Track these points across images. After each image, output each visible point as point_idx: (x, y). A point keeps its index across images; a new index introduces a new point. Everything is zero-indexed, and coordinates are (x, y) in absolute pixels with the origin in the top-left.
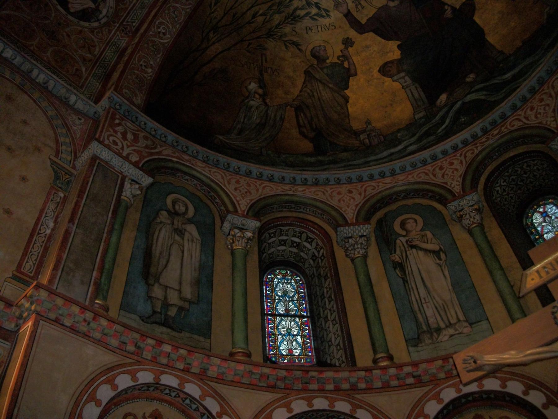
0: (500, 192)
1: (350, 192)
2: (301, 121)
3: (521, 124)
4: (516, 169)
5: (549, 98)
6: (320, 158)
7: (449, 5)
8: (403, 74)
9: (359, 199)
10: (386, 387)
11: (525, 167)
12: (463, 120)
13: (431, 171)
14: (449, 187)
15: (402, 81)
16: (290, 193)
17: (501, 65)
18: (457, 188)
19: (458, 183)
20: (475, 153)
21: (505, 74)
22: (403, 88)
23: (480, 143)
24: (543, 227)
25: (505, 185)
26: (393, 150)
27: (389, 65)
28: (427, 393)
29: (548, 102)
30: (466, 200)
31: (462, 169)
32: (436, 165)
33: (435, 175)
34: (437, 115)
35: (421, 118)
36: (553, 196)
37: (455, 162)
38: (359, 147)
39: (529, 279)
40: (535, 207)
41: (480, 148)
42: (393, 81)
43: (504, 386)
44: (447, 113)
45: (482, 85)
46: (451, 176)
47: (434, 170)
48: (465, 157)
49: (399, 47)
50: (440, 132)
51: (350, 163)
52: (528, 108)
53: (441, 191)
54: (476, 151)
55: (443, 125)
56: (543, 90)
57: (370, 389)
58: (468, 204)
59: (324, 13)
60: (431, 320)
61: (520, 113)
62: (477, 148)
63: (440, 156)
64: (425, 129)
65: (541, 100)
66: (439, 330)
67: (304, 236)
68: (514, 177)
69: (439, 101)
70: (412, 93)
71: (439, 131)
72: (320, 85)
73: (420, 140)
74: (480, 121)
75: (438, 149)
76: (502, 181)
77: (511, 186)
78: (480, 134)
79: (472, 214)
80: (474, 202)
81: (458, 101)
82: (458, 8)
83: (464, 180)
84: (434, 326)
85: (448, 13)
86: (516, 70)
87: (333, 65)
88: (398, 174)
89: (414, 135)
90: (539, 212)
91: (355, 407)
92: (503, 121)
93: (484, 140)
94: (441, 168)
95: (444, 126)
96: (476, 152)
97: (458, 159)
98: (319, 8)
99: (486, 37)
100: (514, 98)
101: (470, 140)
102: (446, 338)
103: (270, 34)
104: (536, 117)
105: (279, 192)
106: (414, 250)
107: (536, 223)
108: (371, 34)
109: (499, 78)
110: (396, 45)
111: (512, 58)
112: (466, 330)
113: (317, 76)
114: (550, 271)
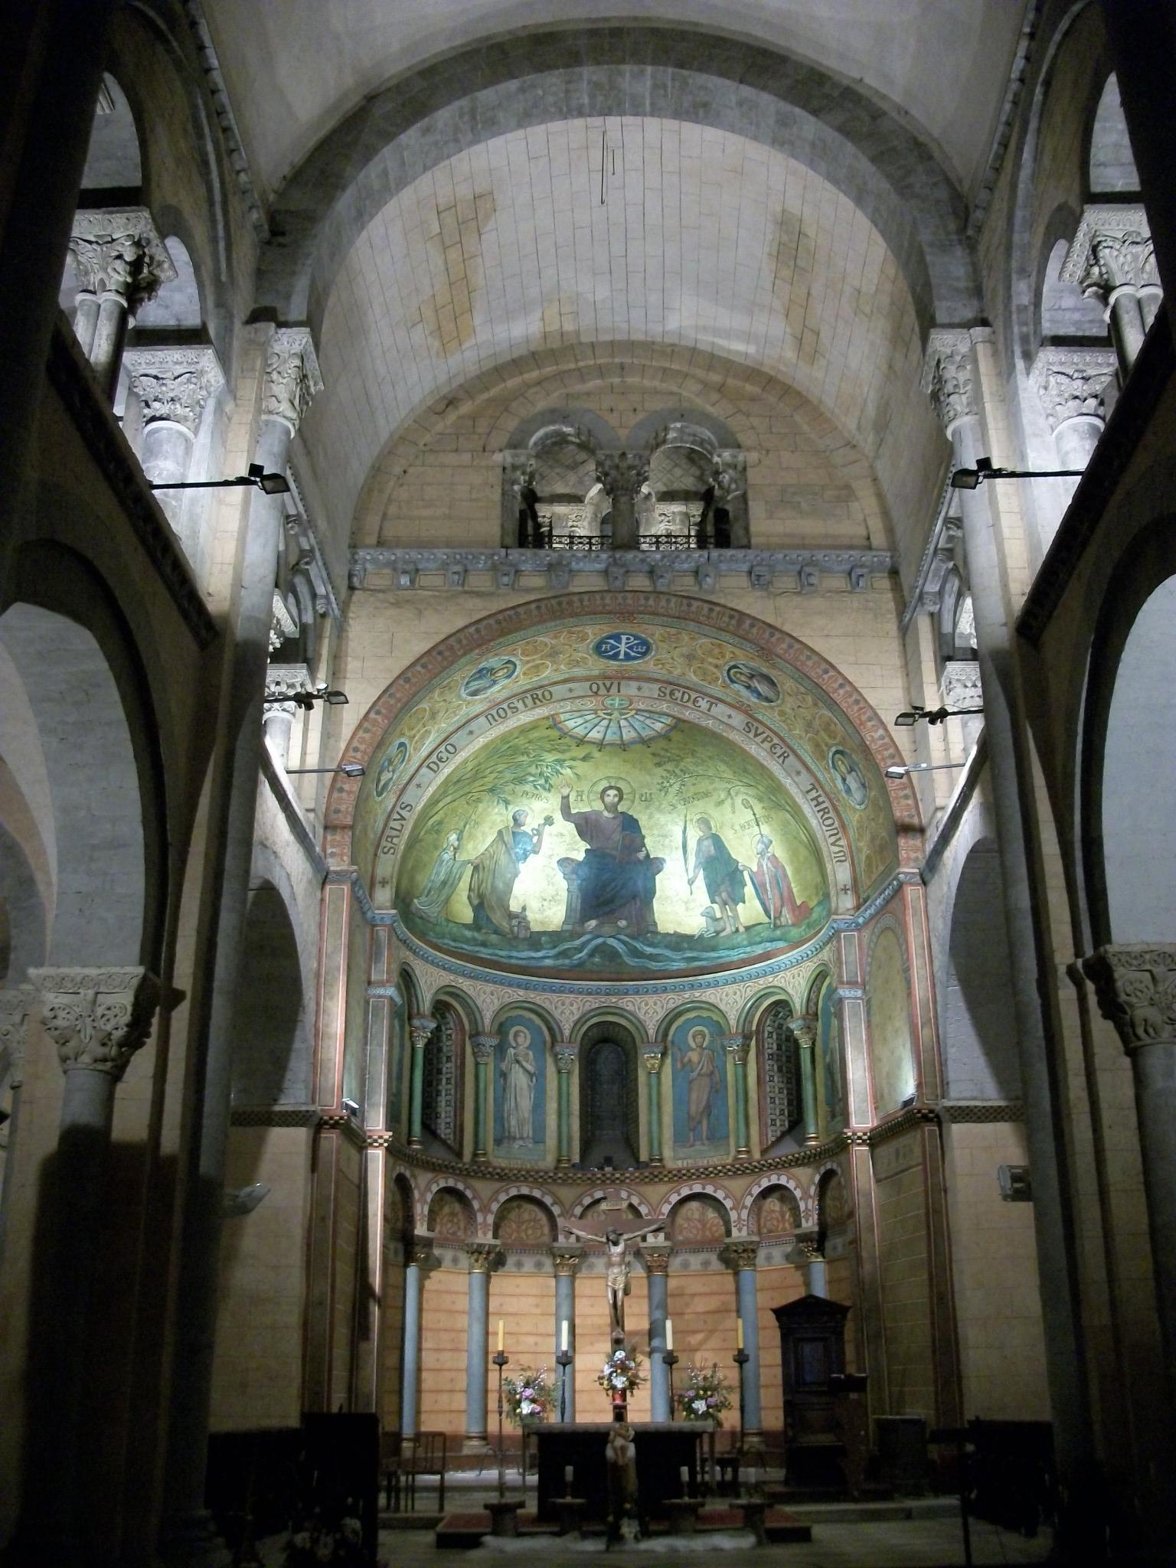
6: (476, 934)
9: (497, 1005)
10: (484, 1177)
26: (533, 954)
35: (567, 931)
41: (597, 1005)
45: (627, 939)
49: (587, 851)
51: (497, 952)
59: (547, 786)
60: (512, 1130)
66: (514, 1139)
73: (557, 956)
85: (641, 855)
87: (525, 834)
89: (555, 947)
91: (467, 1187)
94: (563, 1005)
98: (546, 781)
103: (492, 790)
112: (530, 1146)
113: (506, 839)
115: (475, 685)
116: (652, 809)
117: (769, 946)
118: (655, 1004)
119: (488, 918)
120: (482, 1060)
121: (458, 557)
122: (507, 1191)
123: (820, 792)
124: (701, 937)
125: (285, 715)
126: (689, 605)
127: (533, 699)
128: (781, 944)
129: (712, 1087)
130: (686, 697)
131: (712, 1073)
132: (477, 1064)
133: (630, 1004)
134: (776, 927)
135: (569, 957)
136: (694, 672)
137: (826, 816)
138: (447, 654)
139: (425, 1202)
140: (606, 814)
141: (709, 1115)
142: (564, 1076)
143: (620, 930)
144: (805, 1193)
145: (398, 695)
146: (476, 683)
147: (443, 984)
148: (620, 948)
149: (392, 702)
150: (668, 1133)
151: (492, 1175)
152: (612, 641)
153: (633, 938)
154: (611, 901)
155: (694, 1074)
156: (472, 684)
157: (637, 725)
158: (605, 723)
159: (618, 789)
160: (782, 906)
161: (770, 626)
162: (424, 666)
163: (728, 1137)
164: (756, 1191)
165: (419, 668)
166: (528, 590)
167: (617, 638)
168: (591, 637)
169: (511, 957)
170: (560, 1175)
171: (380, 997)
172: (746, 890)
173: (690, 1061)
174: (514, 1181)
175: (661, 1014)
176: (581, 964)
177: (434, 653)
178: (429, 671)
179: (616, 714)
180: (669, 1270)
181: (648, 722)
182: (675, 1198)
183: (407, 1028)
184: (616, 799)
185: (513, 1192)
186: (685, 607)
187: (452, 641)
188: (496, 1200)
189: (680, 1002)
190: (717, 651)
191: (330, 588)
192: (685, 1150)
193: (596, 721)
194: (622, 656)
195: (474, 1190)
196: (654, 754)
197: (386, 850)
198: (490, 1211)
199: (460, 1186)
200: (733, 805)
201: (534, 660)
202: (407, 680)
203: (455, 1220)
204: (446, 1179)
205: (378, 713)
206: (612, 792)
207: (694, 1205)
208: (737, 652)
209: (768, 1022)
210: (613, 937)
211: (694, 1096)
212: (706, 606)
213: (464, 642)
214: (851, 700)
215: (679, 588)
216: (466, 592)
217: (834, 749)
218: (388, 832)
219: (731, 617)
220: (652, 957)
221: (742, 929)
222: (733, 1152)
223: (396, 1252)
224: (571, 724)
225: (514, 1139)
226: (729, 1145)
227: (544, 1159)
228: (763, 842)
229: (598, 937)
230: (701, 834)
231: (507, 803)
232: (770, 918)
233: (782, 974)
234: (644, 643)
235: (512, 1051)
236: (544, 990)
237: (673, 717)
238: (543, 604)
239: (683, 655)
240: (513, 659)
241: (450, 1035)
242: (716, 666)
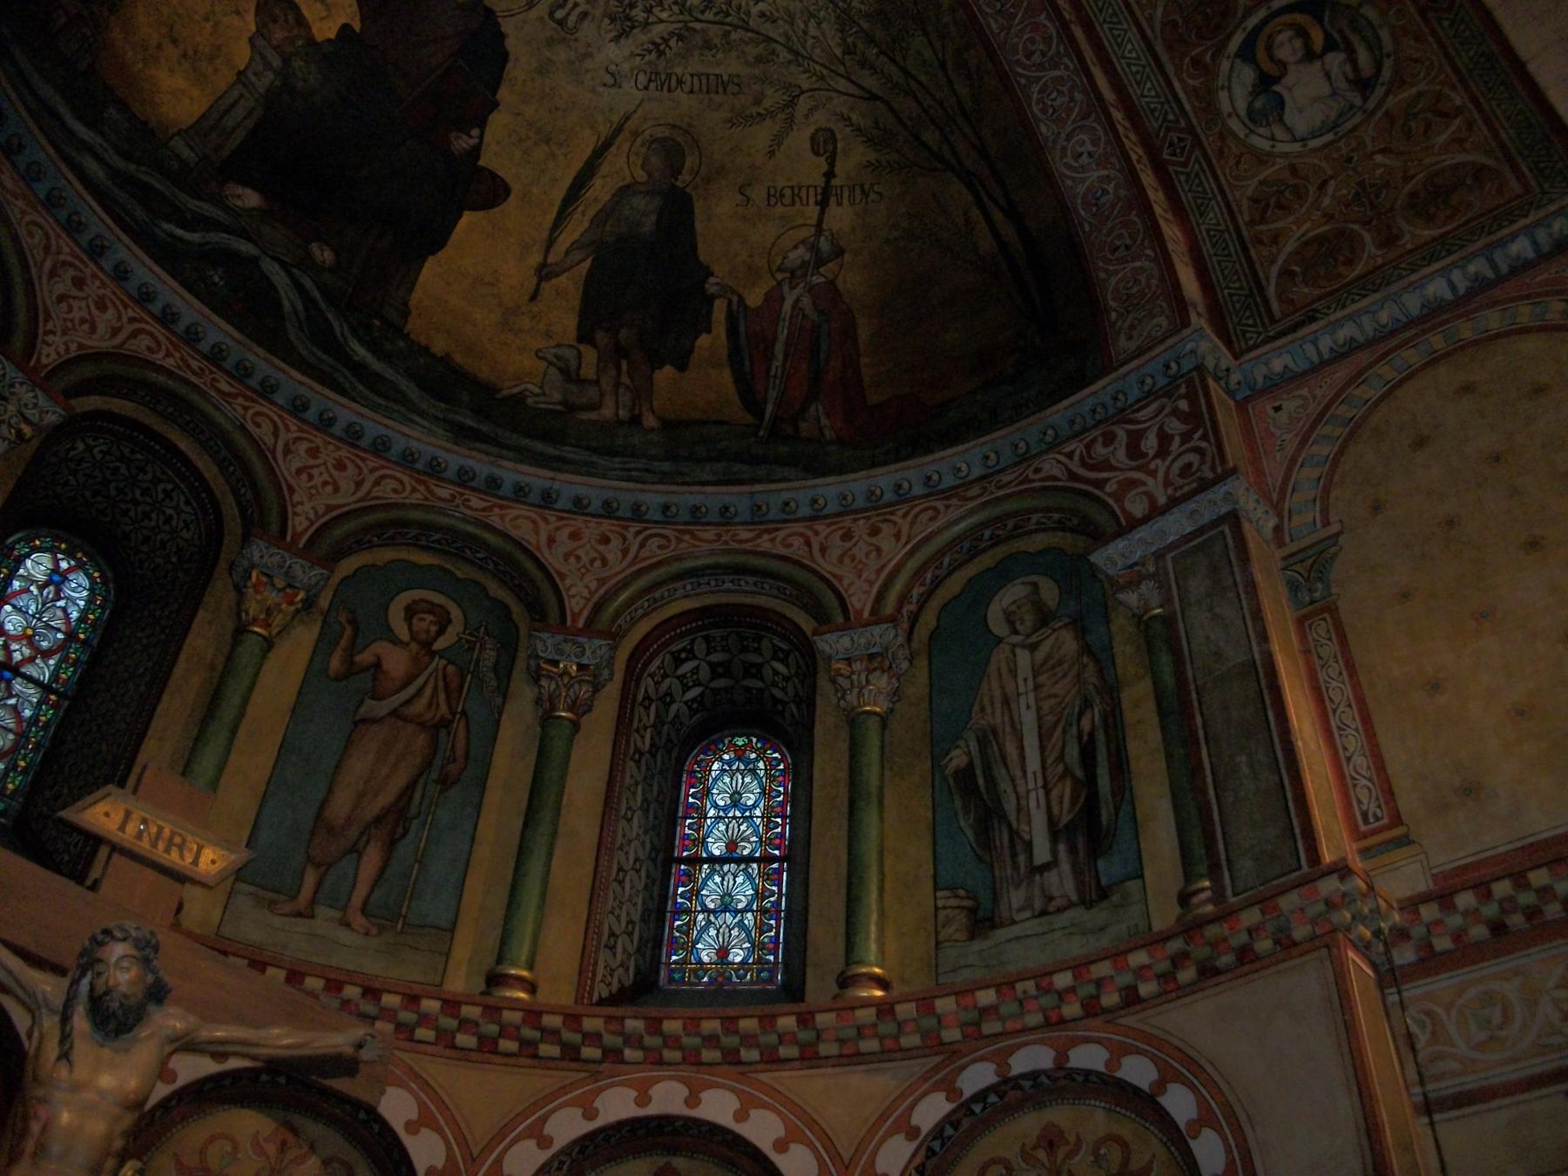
0: (72, 453)
3: (268, 443)
4: (149, 468)
5: (352, 484)
7: (481, 136)
11: (161, 487)
12: (216, 279)
13: (62, 257)
14: (41, 331)
17: (377, 323)
18: (50, 353)
19: (62, 349)
20: (155, 356)
21: (360, 340)
22: (240, 73)
23: (182, 359)
24: (27, 591)
25: (94, 457)
29: (343, 484)
30: (35, 397)
31: (100, 341)
32: (82, 266)
33: (113, 328)
34: (200, 199)
36: (110, 575)
37: (110, 314)
39: (101, 808)
40: (63, 546)
41: (169, 363)
42: (251, 40)
44: (216, 226)
45: (316, 294)
46: (72, 321)
47: (64, 264)
48: (134, 335)
50: (164, 231)
52: (310, 441)
53: (21, 317)
54: (161, 355)
55: (183, 227)
56: (363, 460)
58: (26, 405)
61: (294, 428)
62: (168, 355)
63: (108, 265)
65: (341, 466)
68: (123, 470)
69: (240, 190)
70: (233, 105)
71: (165, 226)
74: (237, 335)
75: (125, 250)
76: (104, 448)
77: (97, 473)
78: (205, 346)
80: (36, 419)
81: (256, 244)
82: (480, 163)
83: (79, 359)
85: (462, 143)
86: (376, 365)
88: (13, 164)
90: (56, 562)
92: (255, 391)
93: (195, 364)
94: (79, 283)
95: (179, 232)
96: (158, 358)
97: (120, 318)
99: (431, 258)
100: (320, 398)
101: (180, 327)
104: (299, 472)
107: (26, 568)
110: (349, 21)
114: (146, 838)
116: (562, 54)
124: (519, 399)
129: (428, 764)
131: (445, 724)
133: (267, 428)
141: (391, 845)
148: (289, 299)
163: (452, 929)
172: (704, 340)
173: (377, 665)
189: (416, 498)
192: (278, 921)
210: (282, 264)
211: (359, 765)
221: (650, 421)
228: (814, 248)
229: (244, 235)
230: (641, 176)
232: (760, 415)
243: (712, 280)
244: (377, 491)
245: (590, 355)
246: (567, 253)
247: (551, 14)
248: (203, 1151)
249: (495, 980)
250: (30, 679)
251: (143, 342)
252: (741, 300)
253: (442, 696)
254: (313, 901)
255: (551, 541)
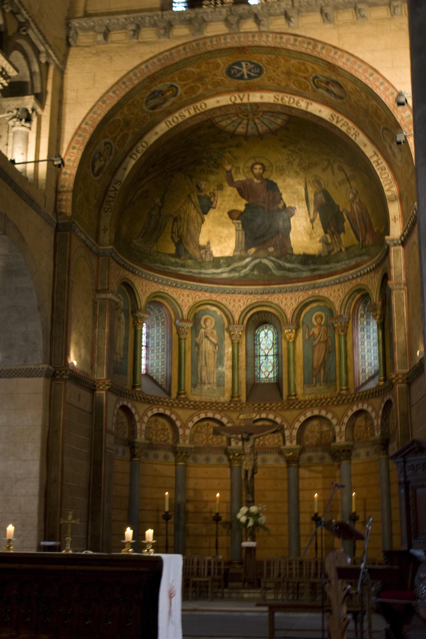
1: (188, 296)
2: (174, 229)
6: (178, 260)
7: (283, 201)
8: (239, 221)
9: (191, 303)
10: (183, 407)
15: (237, 225)
16: (162, 291)
27: (236, 212)
28: (196, 413)
37: (242, 301)
38: (199, 259)
41: (255, 301)
43: (221, 418)
47: (230, 300)
48: (247, 301)
49: (246, 205)
51: (192, 270)
57: (178, 407)
60: (203, 378)
62: (254, 300)
64: (236, 265)
66: (205, 383)
67: (163, 320)
72: (193, 205)
79: (237, 336)
84: (203, 381)
85: (281, 206)
89: (228, 266)
91: (172, 413)
94: (234, 301)
96: (253, 302)
102: (207, 388)
105: (157, 290)
106: (206, 339)
108: (235, 190)
109: (283, 262)
111: (294, 257)
112: (215, 388)
113: (193, 200)
115: (152, 103)
117: (359, 259)
118: (291, 299)
119: (185, 250)
120: (182, 337)
121: (132, 19)
122: (198, 415)
123: (380, 156)
124: (320, 256)
125: (23, 129)
126: (281, 38)
127: (195, 109)
128: (365, 258)
130: (292, 100)
131: (327, 341)
132: (180, 339)
134: (363, 247)
135: (239, 272)
136: (293, 83)
137: (383, 172)
138: (128, 83)
139: (143, 422)
140: (255, 180)
142: (236, 345)
143: (270, 254)
144: (377, 414)
145: (99, 112)
146: (152, 101)
147: (154, 291)
149: (95, 116)
150: (299, 378)
151: (189, 406)
152: (236, 67)
153: (278, 258)
154: (263, 236)
155: (316, 342)
156: (150, 102)
157: (266, 121)
158: (245, 122)
159: (262, 164)
160: (366, 232)
161: (335, 47)
162: (114, 92)
163: (336, 380)
164: (350, 413)
165: (111, 94)
166: (178, 38)
167: (239, 64)
168: (222, 65)
169: (200, 273)
170: (232, 405)
171: (104, 299)
172: (345, 224)
173: (313, 333)
174: (204, 409)
175: (295, 305)
176: (245, 276)
177: (120, 84)
178: (117, 95)
179: (251, 115)
180: (301, 462)
181: (272, 119)
182: (302, 419)
183: (131, 319)
184: (261, 171)
185: (203, 416)
186: (278, 40)
187: (131, 75)
188: (192, 420)
190: (303, 67)
191: (47, 46)
193: (239, 120)
194: (246, 77)
195: (177, 415)
196: (281, 140)
197: (106, 210)
198: (187, 427)
199: (168, 413)
200: (333, 171)
201: (188, 84)
202: (104, 102)
203: (166, 433)
204: (158, 408)
205: (87, 124)
206: (258, 167)
207: (315, 423)
208: (316, 67)
209: (361, 308)
210: (266, 258)
212: (292, 38)
213: (139, 75)
214: (388, 93)
215: (275, 27)
216: (140, 43)
217: (382, 127)
218: (107, 199)
219: (309, 44)
220: (290, 270)
221: (343, 249)
222: (338, 390)
223: (124, 452)
224: (224, 124)
225: (205, 383)
226: (336, 385)
227: (224, 396)
231: (191, 177)
233: (365, 277)
234: (258, 66)
235: (203, 331)
236: (222, 293)
237: (287, 115)
238: (187, 47)
239: (283, 72)
240: (174, 84)
241: (164, 322)
242: (305, 78)
243: (341, 207)
244: (300, 300)
245: (328, 236)
246: (314, 214)
247: (277, 170)
248: (311, 428)
249: (341, 390)
250: (270, 355)
251: (249, 301)
252: (347, 211)
253: (325, 335)
254: (316, 383)
255: (331, 295)
